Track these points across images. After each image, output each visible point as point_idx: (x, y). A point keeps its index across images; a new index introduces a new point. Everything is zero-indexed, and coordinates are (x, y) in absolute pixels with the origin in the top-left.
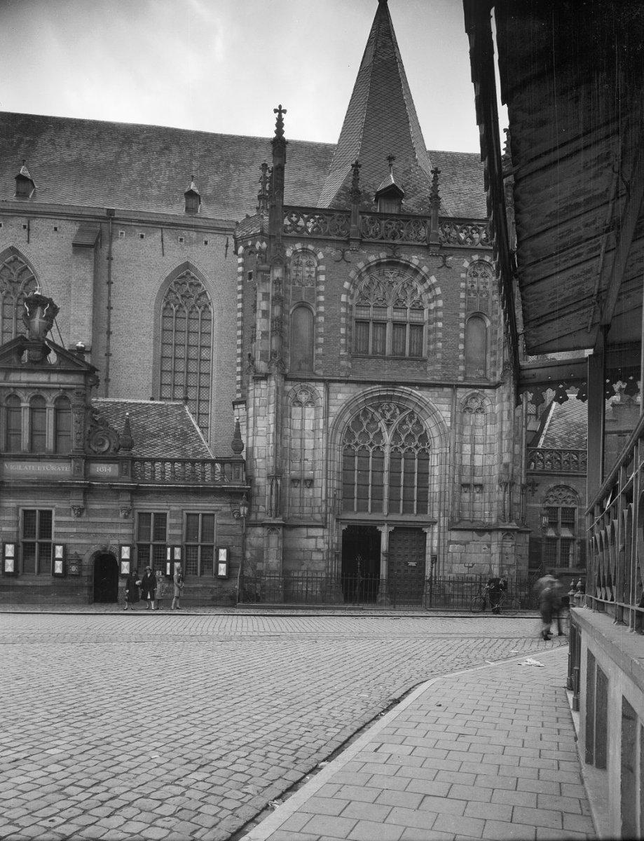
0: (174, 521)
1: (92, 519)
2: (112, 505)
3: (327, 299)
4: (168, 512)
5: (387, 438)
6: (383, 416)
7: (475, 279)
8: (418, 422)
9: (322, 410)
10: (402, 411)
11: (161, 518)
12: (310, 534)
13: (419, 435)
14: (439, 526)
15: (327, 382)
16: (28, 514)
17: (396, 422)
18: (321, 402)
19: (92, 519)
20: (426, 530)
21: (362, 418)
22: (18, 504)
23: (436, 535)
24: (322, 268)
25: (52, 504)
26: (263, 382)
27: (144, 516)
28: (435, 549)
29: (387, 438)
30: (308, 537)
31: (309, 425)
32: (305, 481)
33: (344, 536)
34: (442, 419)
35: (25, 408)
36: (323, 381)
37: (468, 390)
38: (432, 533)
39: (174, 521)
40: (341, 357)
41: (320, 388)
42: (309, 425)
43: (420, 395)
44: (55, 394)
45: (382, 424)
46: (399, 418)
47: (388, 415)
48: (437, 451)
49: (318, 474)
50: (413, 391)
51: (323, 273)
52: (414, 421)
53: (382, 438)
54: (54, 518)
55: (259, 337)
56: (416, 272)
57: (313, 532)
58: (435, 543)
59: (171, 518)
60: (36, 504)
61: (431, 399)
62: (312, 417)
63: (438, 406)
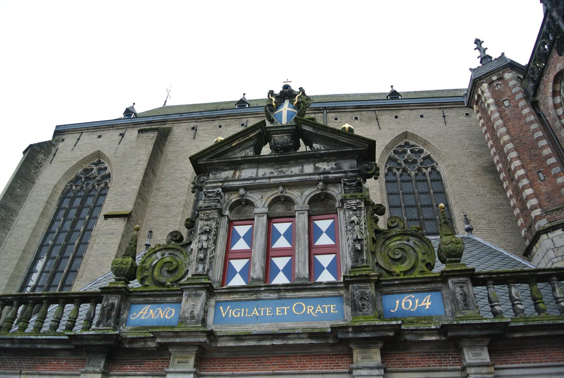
35: (260, 214)
44: (309, 192)
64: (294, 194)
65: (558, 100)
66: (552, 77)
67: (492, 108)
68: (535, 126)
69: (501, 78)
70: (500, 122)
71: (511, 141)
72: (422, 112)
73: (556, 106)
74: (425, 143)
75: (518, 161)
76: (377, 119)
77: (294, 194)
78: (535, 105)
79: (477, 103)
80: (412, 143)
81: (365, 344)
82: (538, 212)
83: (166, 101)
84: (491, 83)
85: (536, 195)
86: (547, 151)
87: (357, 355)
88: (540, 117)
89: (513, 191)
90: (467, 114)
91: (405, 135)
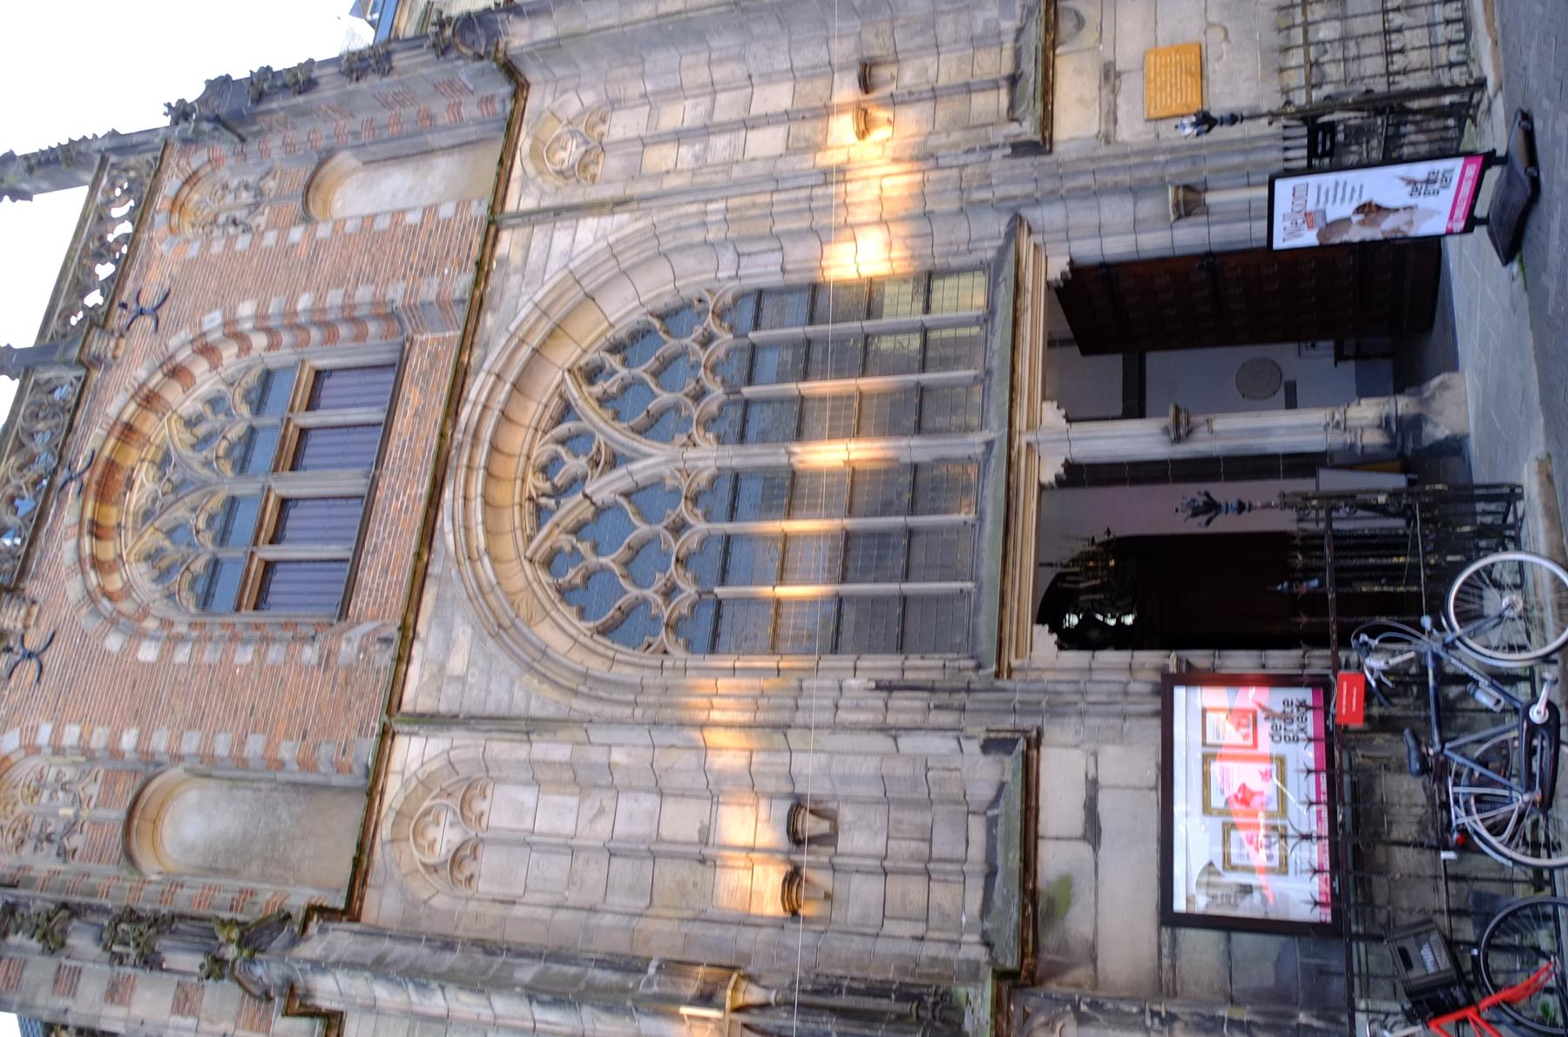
5: (654, 460)
6: (576, 482)
7: (222, 219)
8: (615, 348)
10: (567, 411)
12: (1077, 823)
13: (664, 337)
15: (393, 718)
17: (610, 432)
21: (573, 575)
23: (1082, 215)
24: (44, 734)
29: (654, 460)
30: (1092, 831)
31: (557, 814)
32: (795, 838)
33: (1070, 648)
34: (603, 244)
37: (517, 172)
38: (1067, 234)
40: (326, 660)
42: (557, 814)
43: (503, 341)
45: (605, 487)
46: (593, 417)
47: (574, 464)
48: (728, 257)
50: (486, 366)
51: (57, 732)
52: (613, 361)
53: (656, 484)
57: (1060, 806)
58: (1116, 211)
61: (524, 298)
62: (528, 796)
63: (554, 265)
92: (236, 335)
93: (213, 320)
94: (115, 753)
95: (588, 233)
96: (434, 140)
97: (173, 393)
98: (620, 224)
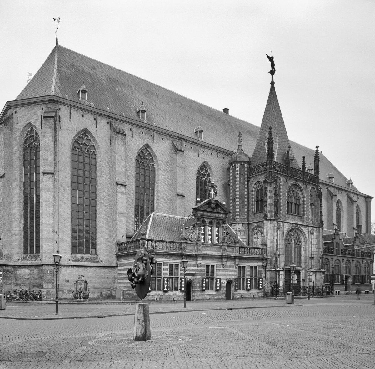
0: (248, 269)
1: (227, 269)
2: (232, 264)
3: (283, 194)
4: (246, 266)
9: (282, 232)
11: (244, 267)
14: (305, 270)
16: (208, 266)
18: (282, 229)
19: (227, 269)
20: (300, 271)
22: (206, 263)
25: (217, 263)
26: (269, 221)
27: (240, 267)
28: (303, 278)
36: (283, 222)
39: (248, 269)
41: (282, 224)
49: (281, 253)
54: (215, 268)
55: (268, 205)
56: (300, 188)
58: (304, 275)
59: (247, 268)
60: (211, 263)
64: (213, 221)
65: (255, 186)
66: (257, 180)
67: (238, 176)
68: (246, 190)
69: (244, 165)
70: (238, 183)
71: (239, 191)
72: (212, 152)
73: (254, 188)
74: (210, 168)
75: (239, 199)
76: (198, 151)
77: (213, 221)
78: (248, 181)
79: (233, 166)
80: (206, 166)
81: (225, 258)
82: (238, 217)
83: (57, 38)
84: (241, 165)
85: (239, 212)
86: (246, 200)
87: (223, 259)
88: (248, 188)
89: (233, 205)
90: (224, 158)
91: (205, 162)
92: (303, 197)
93: (305, 195)
94: (281, 192)
95: (307, 235)
96: (313, 217)
97: (300, 190)
98: (307, 238)
